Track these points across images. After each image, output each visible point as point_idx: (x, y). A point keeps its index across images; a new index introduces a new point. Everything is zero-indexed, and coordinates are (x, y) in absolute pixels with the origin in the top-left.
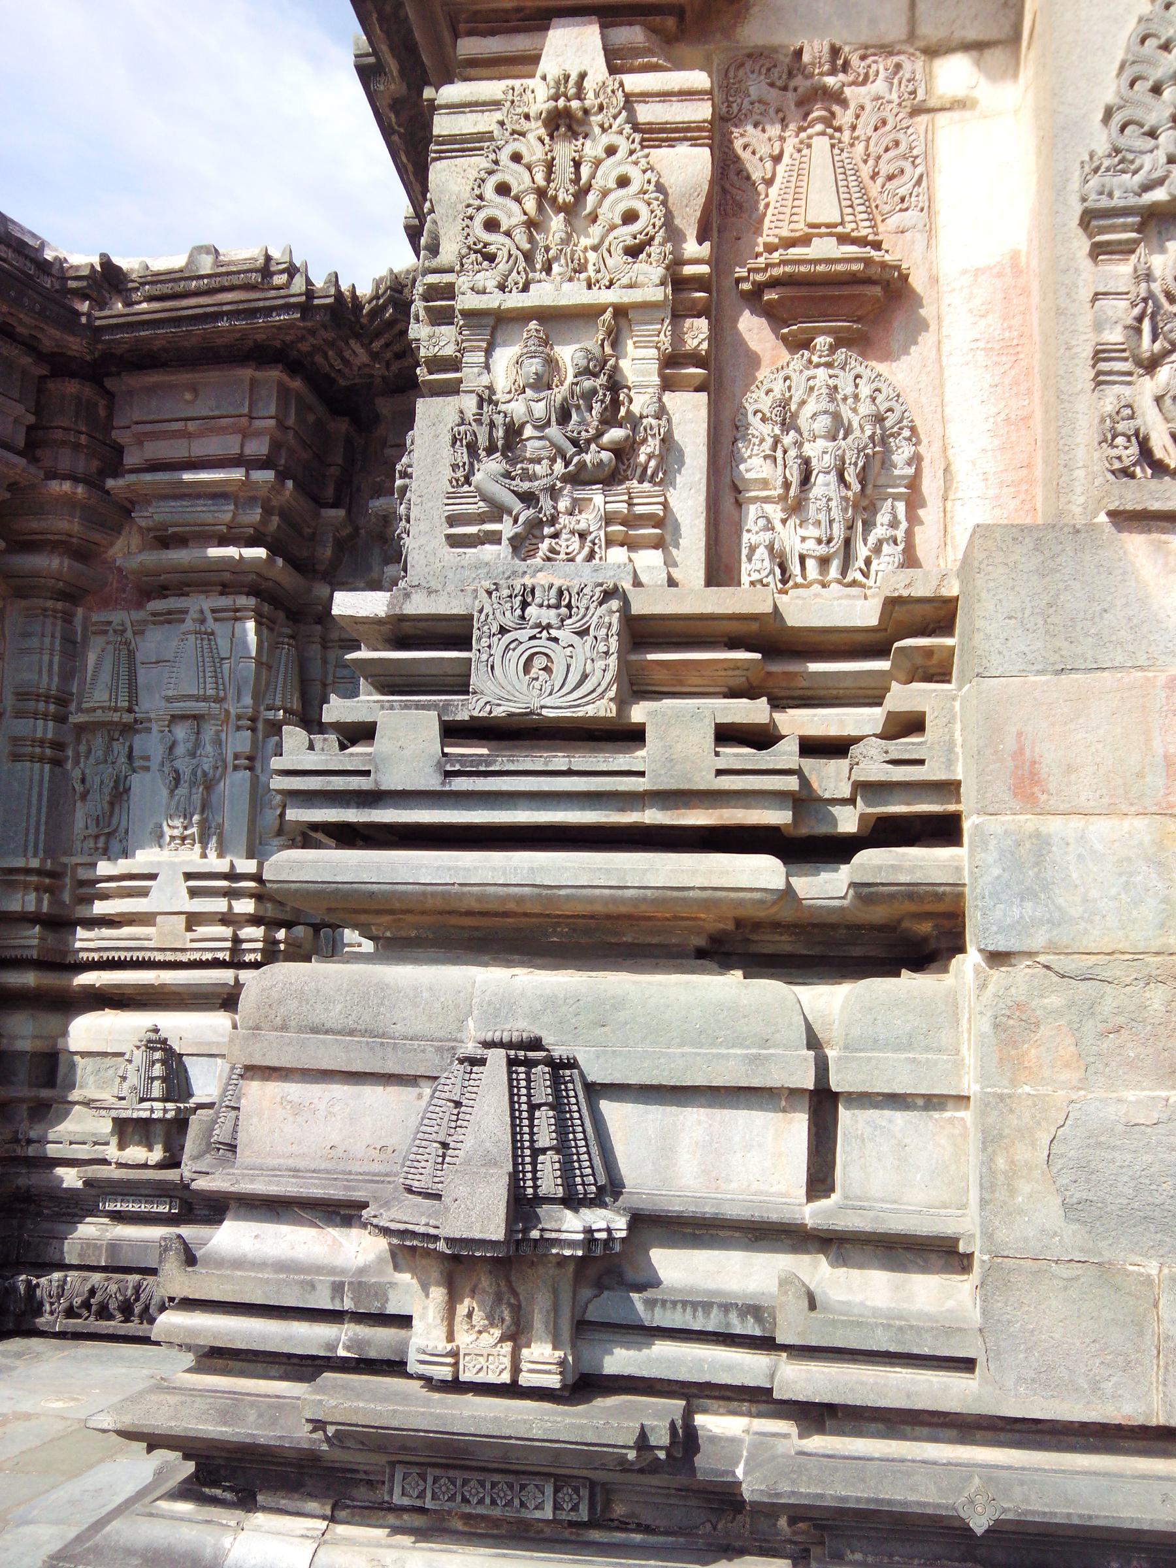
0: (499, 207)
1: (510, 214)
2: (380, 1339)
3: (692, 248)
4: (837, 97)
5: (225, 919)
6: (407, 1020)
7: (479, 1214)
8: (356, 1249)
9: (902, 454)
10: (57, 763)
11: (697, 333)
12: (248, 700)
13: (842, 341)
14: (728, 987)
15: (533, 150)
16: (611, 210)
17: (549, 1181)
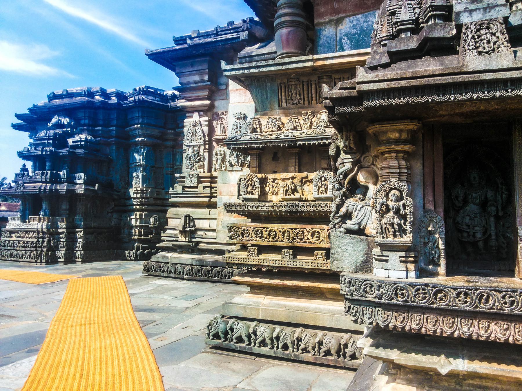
1: (190, 135)
6: (180, 213)
11: (207, 146)
13: (222, 145)
16: (198, 135)
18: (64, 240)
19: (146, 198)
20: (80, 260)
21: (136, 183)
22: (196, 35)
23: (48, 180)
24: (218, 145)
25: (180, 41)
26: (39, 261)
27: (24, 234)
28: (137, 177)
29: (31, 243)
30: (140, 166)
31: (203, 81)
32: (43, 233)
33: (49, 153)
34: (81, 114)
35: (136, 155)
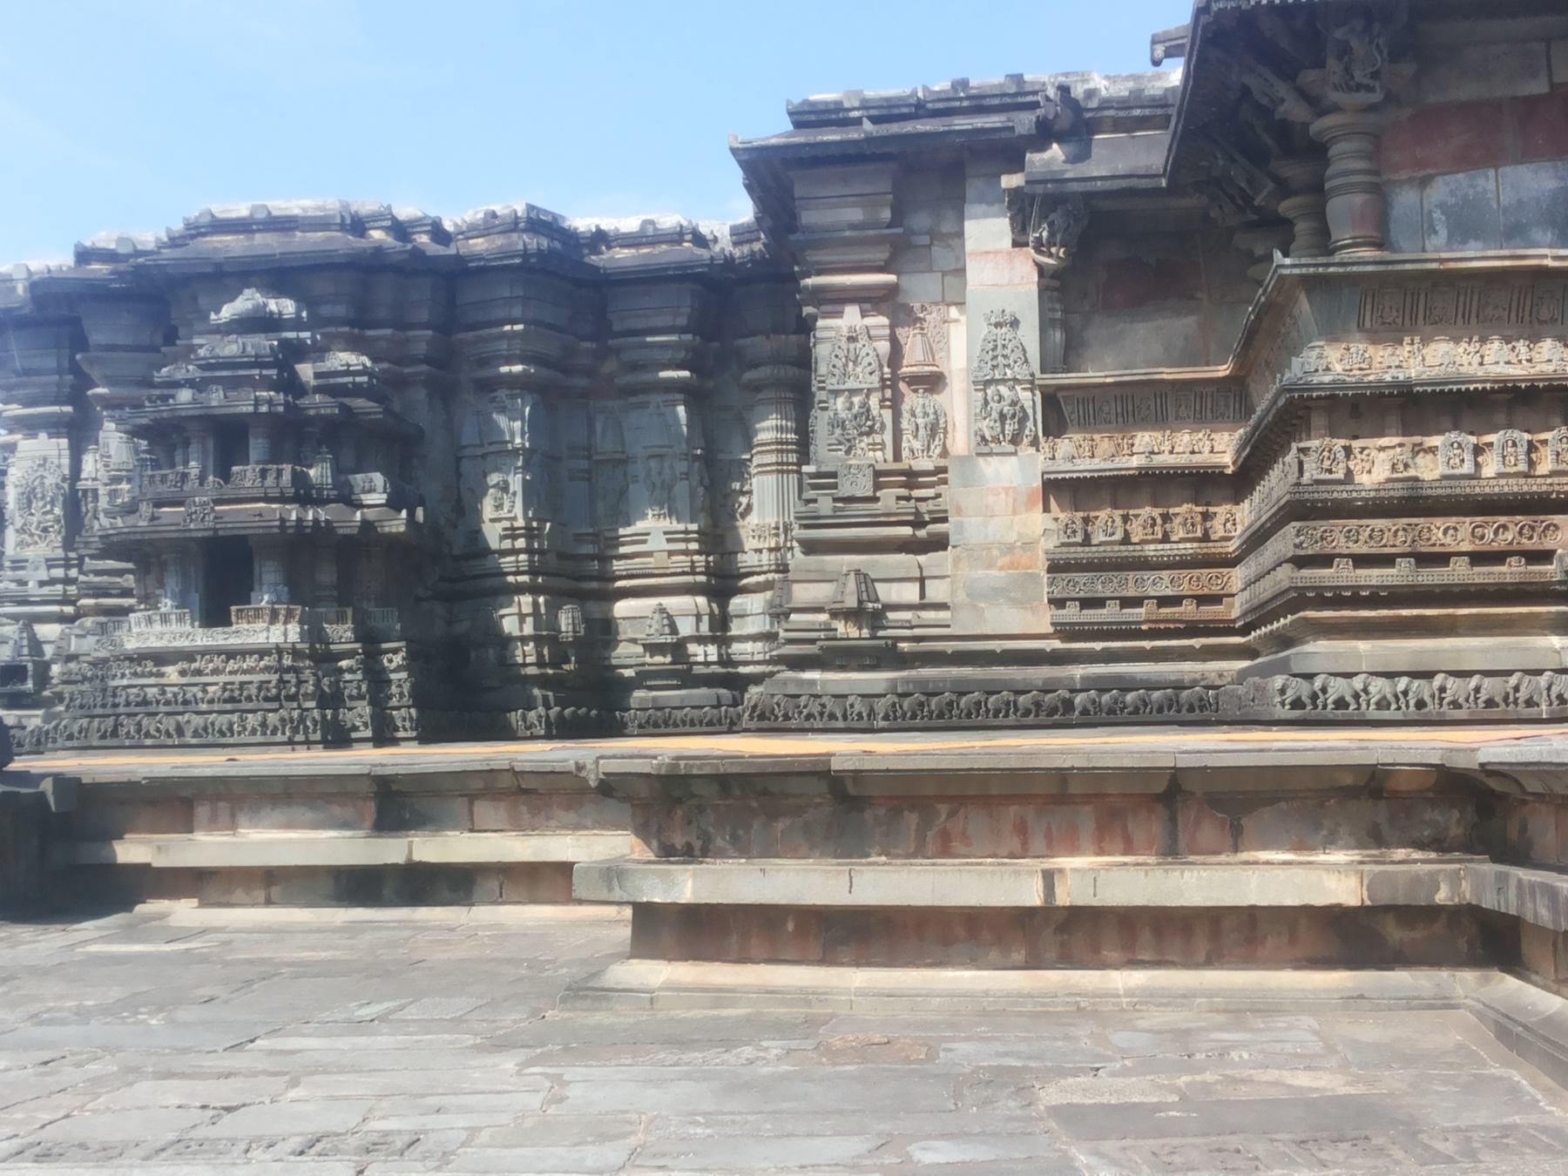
0: (835, 361)
1: (839, 364)
2: (831, 634)
3: (886, 370)
4: (922, 320)
5: (685, 552)
7: (852, 602)
8: (824, 617)
9: (942, 421)
10: (589, 480)
11: (888, 393)
12: (684, 446)
13: (926, 390)
14: (902, 557)
15: (844, 346)
16: (865, 362)
17: (865, 597)
18: (359, 676)
19: (541, 552)
20: (414, 734)
21: (499, 507)
22: (857, 104)
23: (291, 492)
24: (915, 391)
25: (807, 117)
26: (299, 737)
27: (218, 662)
28: (505, 488)
29: (260, 689)
30: (515, 452)
31: (876, 225)
32: (296, 653)
33: (281, 409)
34: (322, 286)
35: (502, 421)
